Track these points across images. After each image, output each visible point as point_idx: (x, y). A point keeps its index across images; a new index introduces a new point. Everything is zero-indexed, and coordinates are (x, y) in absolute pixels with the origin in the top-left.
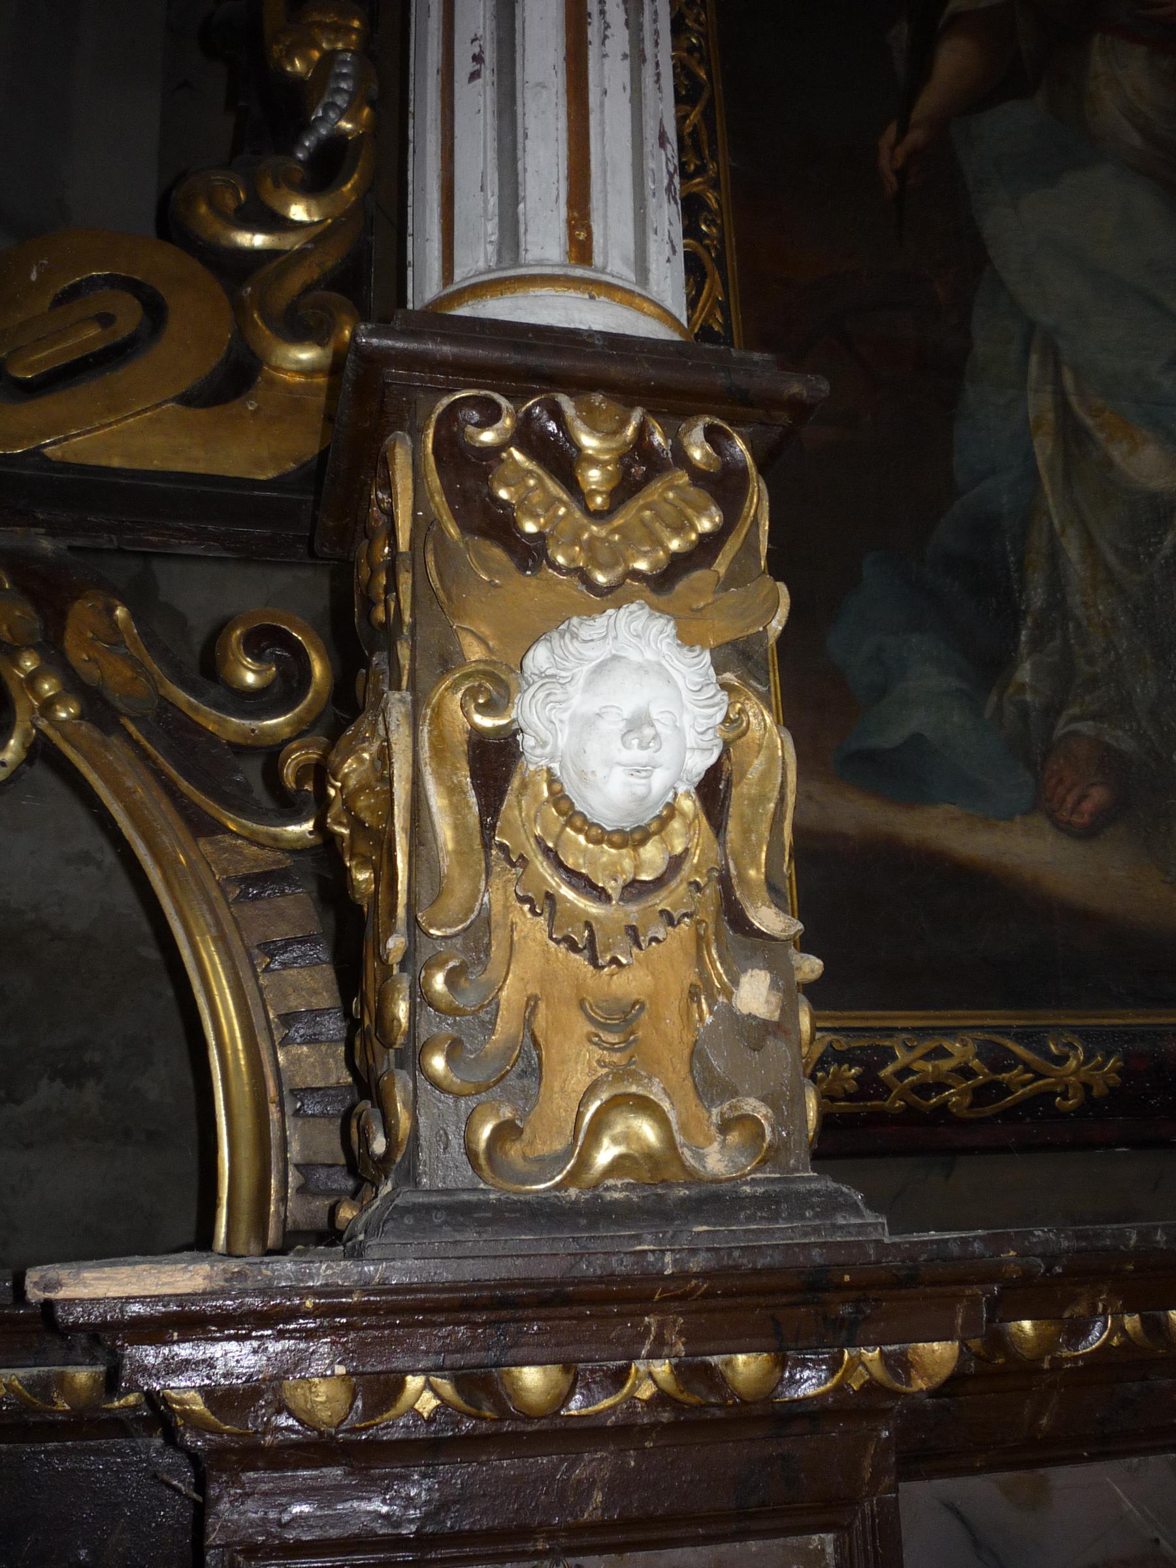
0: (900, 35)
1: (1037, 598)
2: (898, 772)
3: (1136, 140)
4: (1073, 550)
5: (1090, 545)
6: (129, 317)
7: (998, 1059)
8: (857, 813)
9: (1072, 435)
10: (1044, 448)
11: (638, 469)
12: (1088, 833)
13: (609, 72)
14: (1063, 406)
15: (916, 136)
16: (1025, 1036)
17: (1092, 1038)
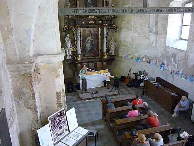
9: (87, 49)
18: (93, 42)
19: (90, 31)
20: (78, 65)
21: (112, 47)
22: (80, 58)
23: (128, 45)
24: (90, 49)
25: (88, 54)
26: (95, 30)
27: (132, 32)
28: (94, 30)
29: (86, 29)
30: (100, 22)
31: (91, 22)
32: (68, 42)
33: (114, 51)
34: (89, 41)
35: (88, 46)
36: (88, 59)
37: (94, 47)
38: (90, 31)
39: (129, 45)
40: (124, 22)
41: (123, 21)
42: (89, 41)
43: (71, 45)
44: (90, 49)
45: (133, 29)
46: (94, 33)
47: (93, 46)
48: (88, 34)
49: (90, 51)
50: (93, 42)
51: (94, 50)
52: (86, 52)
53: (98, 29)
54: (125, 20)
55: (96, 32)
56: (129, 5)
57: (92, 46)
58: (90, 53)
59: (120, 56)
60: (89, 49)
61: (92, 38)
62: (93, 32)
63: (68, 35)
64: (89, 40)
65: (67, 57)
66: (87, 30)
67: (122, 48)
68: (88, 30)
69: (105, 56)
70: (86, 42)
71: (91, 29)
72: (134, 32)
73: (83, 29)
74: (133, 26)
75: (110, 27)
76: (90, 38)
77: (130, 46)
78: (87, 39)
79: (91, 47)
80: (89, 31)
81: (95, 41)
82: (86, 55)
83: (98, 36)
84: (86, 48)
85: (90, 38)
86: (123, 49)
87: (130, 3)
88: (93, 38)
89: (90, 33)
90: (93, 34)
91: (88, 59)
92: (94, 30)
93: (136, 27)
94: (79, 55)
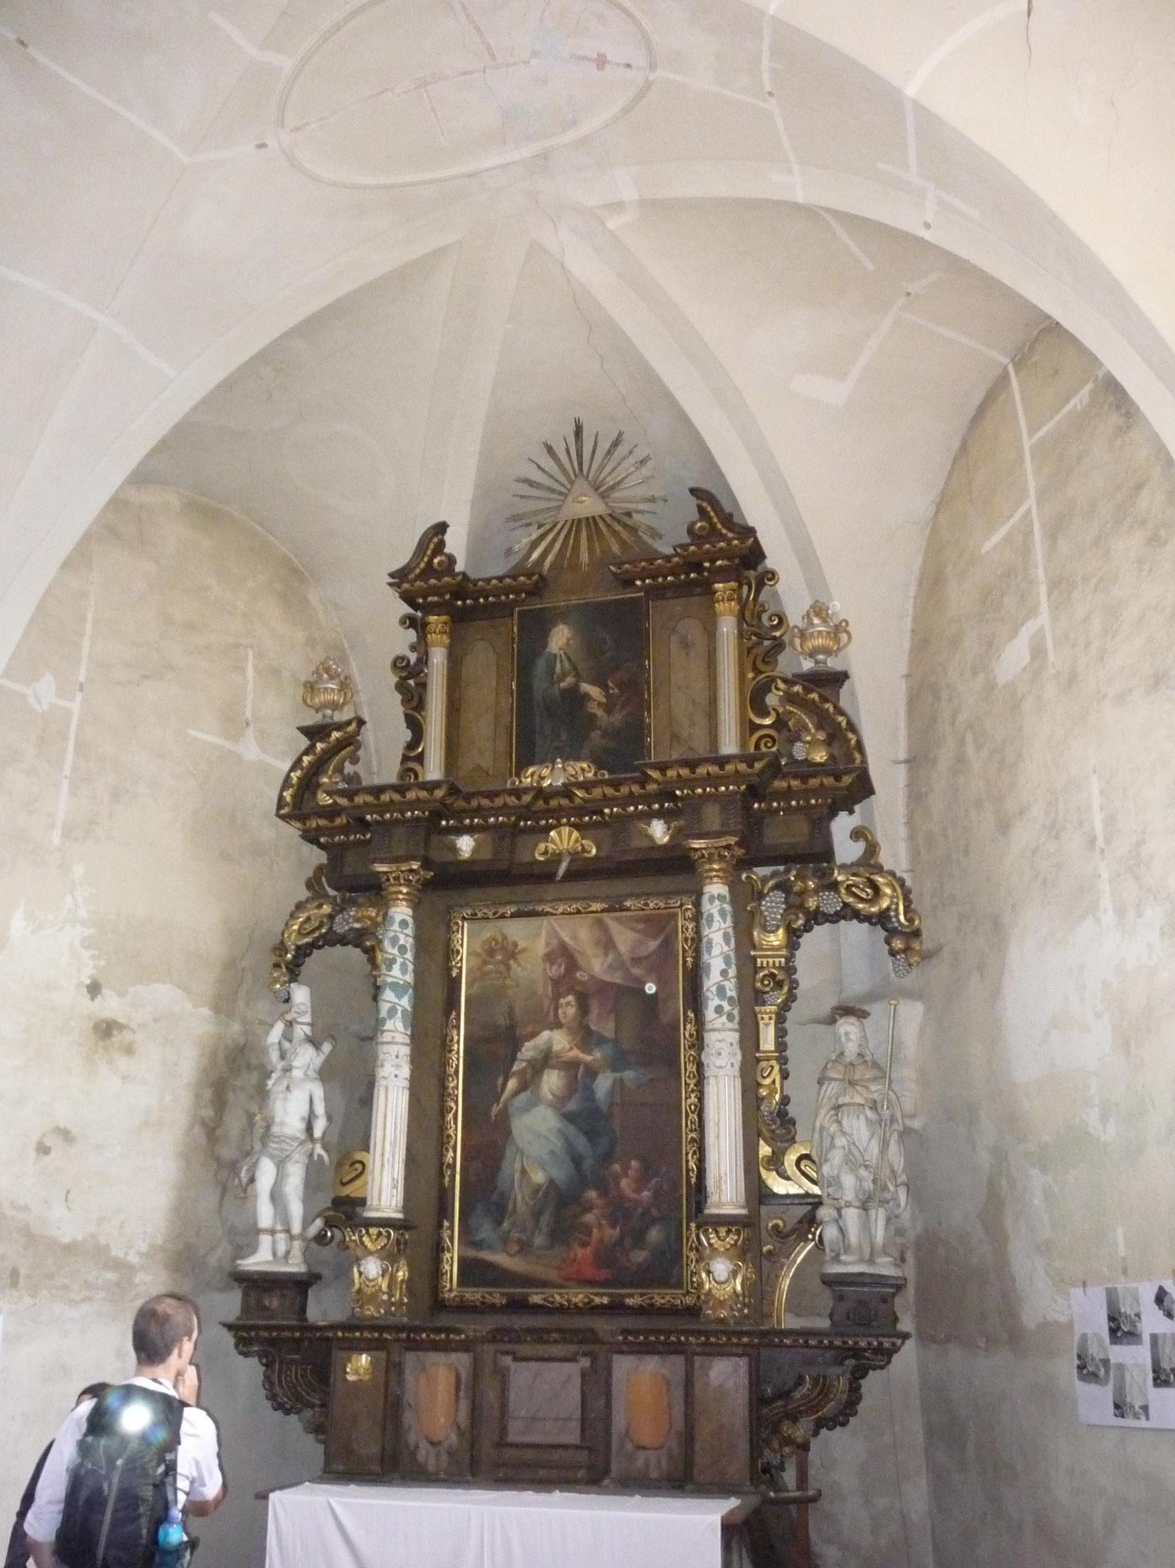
0: (500, 1081)
1: (511, 1207)
2: (479, 1245)
3: (550, 1097)
4: (519, 1198)
5: (523, 1198)
6: (359, 1166)
7: (483, 1297)
8: (471, 1253)
9: (524, 1172)
10: (517, 1176)
11: (380, 1234)
12: (511, 1256)
13: (385, 1173)
14: (523, 1167)
15: (501, 1105)
16: (490, 1294)
17: (502, 1294)
18: (603, 1084)
19: (564, 954)
20: (337, 1355)
21: (852, 1162)
22: (372, 1267)
23: (1092, 1117)
24: (561, 1173)
25: (524, 1248)
26: (625, 938)
27: (1108, 918)
28: (608, 944)
29: (517, 931)
30: (659, 831)
31: (563, 839)
32: (287, 1070)
33: (879, 1217)
34: (552, 1081)
35: (538, 1134)
36: (518, 1305)
37: (608, 1157)
38: (564, 954)
39: (1104, 1119)
40: (1023, 835)
41: (1004, 827)
42: (552, 1081)
43: (320, 1109)
44: (551, 1182)
45: (1105, 875)
46: (617, 978)
47: (591, 1135)
48: (544, 990)
49: (562, 1206)
50: (603, 1084)
51: (603, 1190)
52: (499, 1210)
53: (660, 925)
54: (1022, 812)
55: (636, 961)
56: (1031, 627)
57: (581, 1143)
58: (561, 1234)
59: (1029, 1318)
60: (539, 1177)
61: (586, 1037)
62: (597, 965)
63: (301, 995)
64: (546, 1060)
65: (253, 1249)
66: (531, 939)
67: (1037, 1181)
68: (541, 948)
69: (721, 1267)
70: (512, 1084)
71: (578, 933)
72: (1120, 912)
73: (488, 931)
74: (1108, 841)
75: (812, 903)
76: (559, 1041)
77: (1109, 1133)
78: (528, 1050)
79: (576, 1161)
80: (549, 958)
81: (629, 1075)
82: (501, 1259)
83: (665, 1019)
84: (512, 1167)
85: (559, 1041)
86: (1047, 1195)
87: (1043, 590)
88: (601, 1040)
89: (560, 986)
90: (603, 988)
91: (518, 1305)
92: (608, 944)
93: (1140, 843)
94: (369, 1223)
